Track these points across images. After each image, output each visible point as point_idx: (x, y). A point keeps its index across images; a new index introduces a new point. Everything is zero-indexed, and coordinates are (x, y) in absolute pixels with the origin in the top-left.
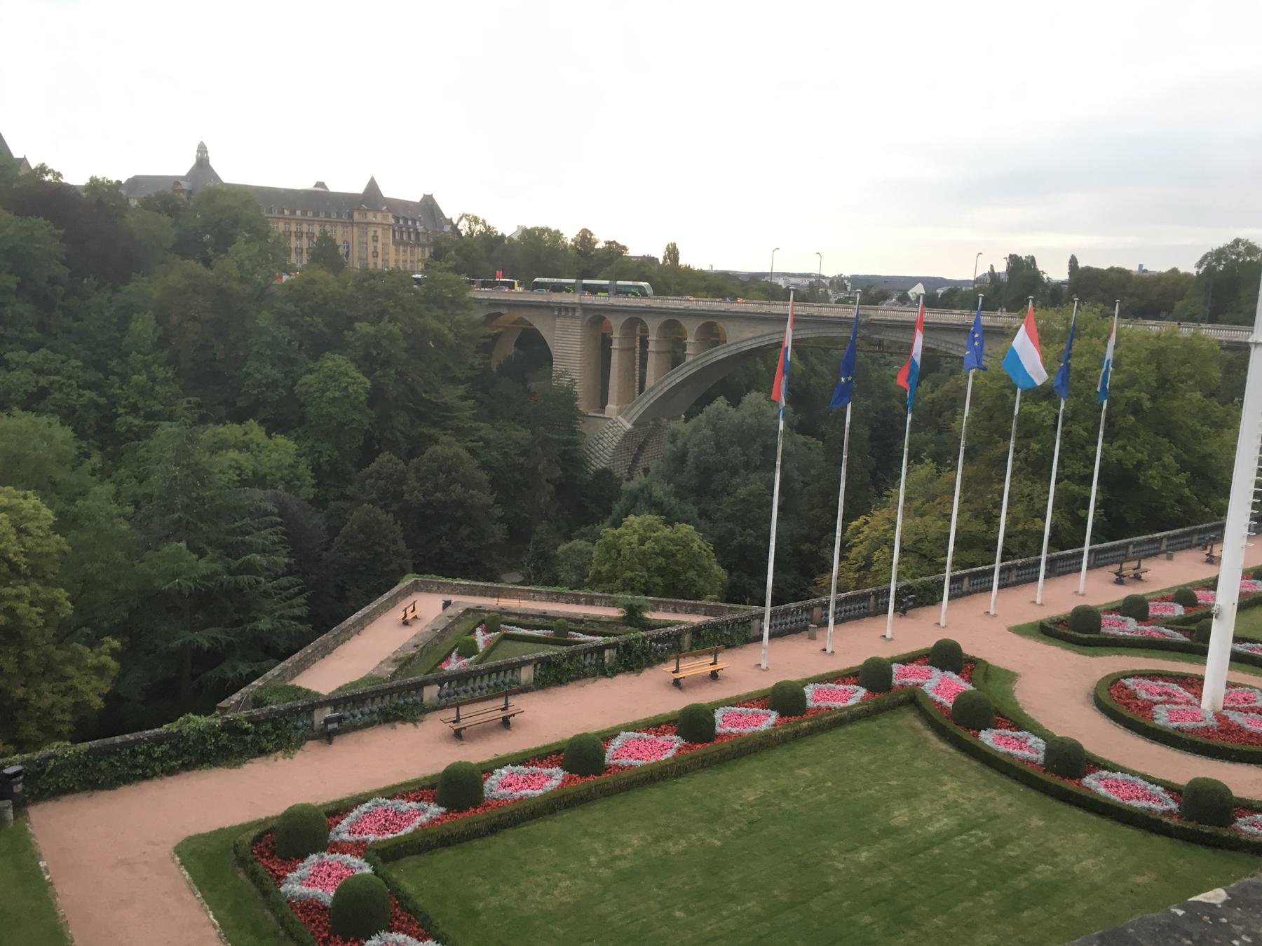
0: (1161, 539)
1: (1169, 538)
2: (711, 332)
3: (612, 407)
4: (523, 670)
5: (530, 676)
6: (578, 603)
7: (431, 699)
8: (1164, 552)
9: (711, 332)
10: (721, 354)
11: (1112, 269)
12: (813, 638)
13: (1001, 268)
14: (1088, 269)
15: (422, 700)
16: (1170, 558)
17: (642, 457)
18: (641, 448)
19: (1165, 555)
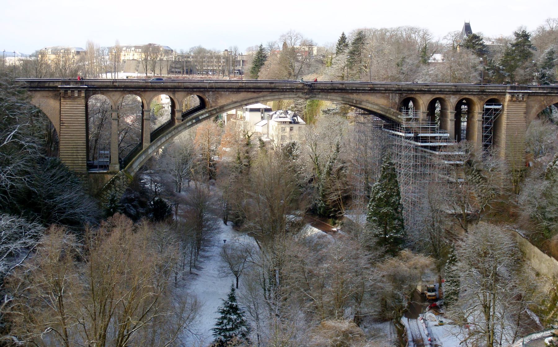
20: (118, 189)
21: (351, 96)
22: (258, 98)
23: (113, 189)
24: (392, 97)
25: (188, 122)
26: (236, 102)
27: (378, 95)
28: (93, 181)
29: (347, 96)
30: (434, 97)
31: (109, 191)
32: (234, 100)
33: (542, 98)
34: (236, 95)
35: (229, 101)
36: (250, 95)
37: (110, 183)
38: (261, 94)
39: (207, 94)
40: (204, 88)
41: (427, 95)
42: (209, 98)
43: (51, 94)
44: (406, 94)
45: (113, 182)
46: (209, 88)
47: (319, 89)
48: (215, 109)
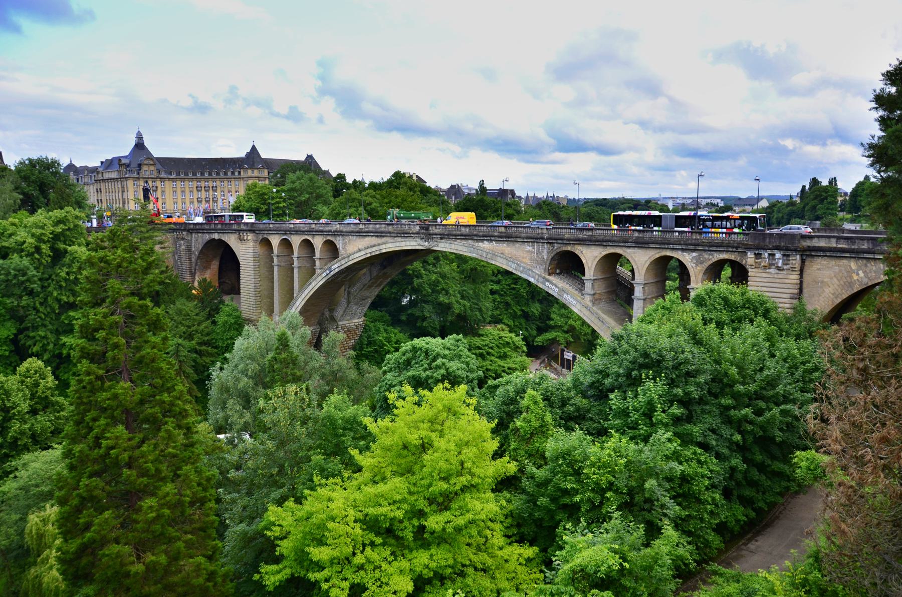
9: (332, 250)
10: (336, 267)
21: (481, 244)
22: (379, 245)
24: (538, 249)
27: (517, 245)
30: (604, 253)
32: (361, 247)
33: (853, 264)
34: (362, 240)
35: (356, 249)
38: (384, 239)
39: (338, 238)
41: (593, 248)
42: (339, 242)
43: (236, 236)
44: (559, 245)
47: (436, 234)
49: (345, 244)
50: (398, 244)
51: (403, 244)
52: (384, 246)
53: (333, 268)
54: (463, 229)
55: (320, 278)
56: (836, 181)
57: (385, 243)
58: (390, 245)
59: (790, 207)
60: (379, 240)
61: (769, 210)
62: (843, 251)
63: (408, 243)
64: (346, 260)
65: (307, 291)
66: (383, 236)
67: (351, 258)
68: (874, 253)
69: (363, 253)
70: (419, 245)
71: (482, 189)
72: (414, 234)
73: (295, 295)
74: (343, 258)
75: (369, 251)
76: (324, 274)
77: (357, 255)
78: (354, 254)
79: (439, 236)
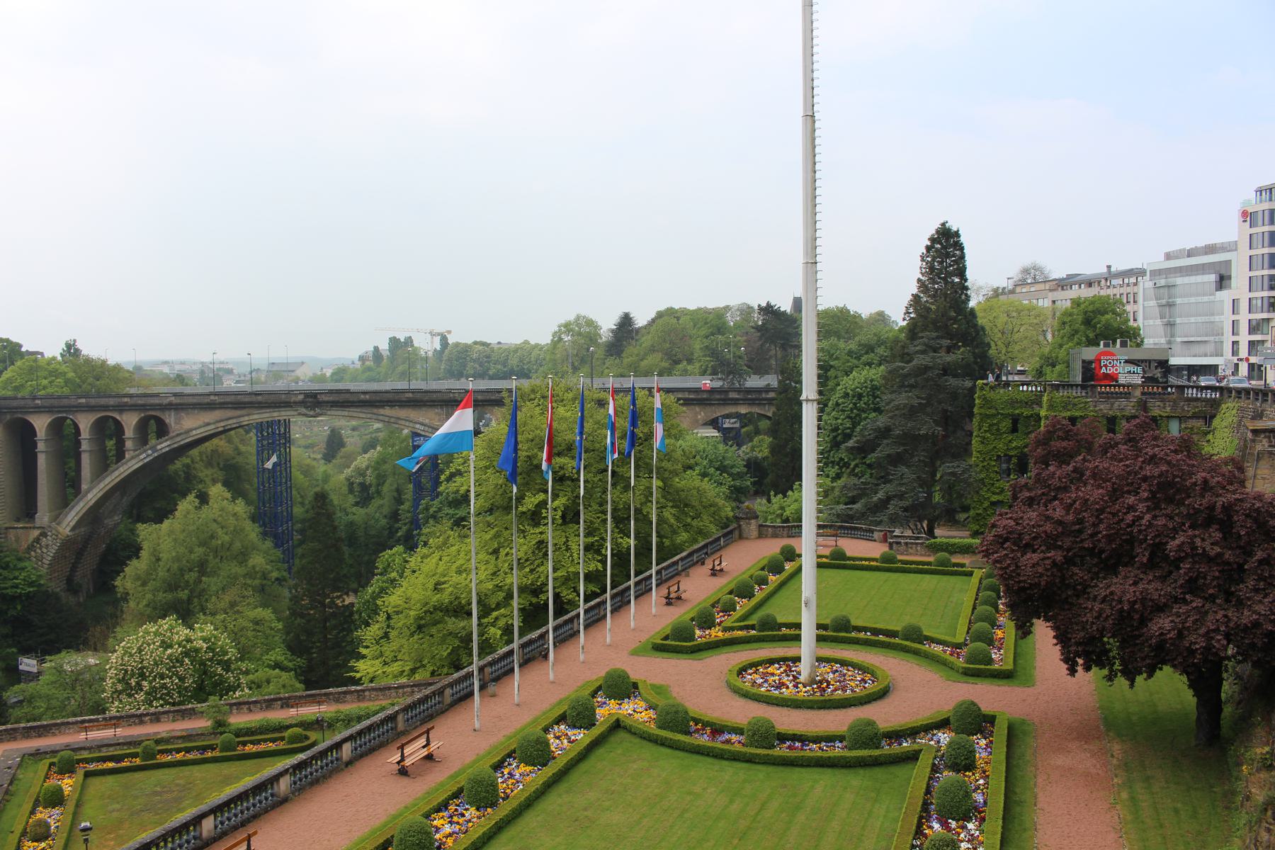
0: (678, 560)
1: (682, 559)
2: (153, 425)
3: (43, 516)
4: (282, 780)
5: (287, 786)
6: (142, 723)
7: (209, 831)
8: (683, 570)
9: (153, 425)
10: (164, 446)
11: (475, 343)
12: (494, 696)
13: (384, 346)
14: (457, 345)
15: (201, 834)
16: (688, 575)
17: (79, 566)
18: (80, 554)
19: (683, 573)
20: (45, 550)
21: (381, 411)
22: (239, 417)
23: (38, 551)
25: (141, 454)
26: (208, 424)
27: (424, 409)
28: (13, 539)
29: (375, 411)
31: (33, 553)
32: (207, 421)
33: (697, 409)
35: (199, 423)
36: (229, 413)
37: (34, 542)
39: (167, 413)
40: (160, 405)
42: (170, 419)
45: (37, 540)
46: (166, 405)
47: (328, 402)
48: (178, 435)
49: (178, 421)
50: (267, 415)
51: (275, 414)
52: (246, 418)
53: (159, 447)
54: (362, 396)
55: (134, 462)
56: (412, 342)
57: (248, 415)
58: (255, 417)
59: (368, 373)
60: (238, 413)
61: (335, 377)
62: (693, 399)
63: (283, 413)
64: (183, 436)
65: (108, 479)
66: (245, 408)
67: (194, 432)
68: (711, 400)
69: (213, 427)
70: (300, 414)
71: (71, 350)
72: (295, 403)
73: (84, 487)
74: (178, 435)
75: (222, 424)
76: (144, 455)
77: (198, 431)
78: (195, 429)
79: (329, 404)
